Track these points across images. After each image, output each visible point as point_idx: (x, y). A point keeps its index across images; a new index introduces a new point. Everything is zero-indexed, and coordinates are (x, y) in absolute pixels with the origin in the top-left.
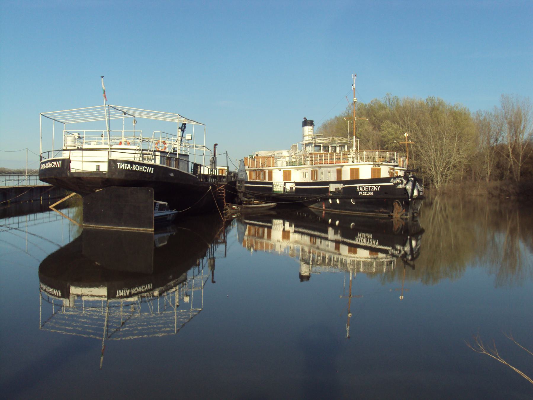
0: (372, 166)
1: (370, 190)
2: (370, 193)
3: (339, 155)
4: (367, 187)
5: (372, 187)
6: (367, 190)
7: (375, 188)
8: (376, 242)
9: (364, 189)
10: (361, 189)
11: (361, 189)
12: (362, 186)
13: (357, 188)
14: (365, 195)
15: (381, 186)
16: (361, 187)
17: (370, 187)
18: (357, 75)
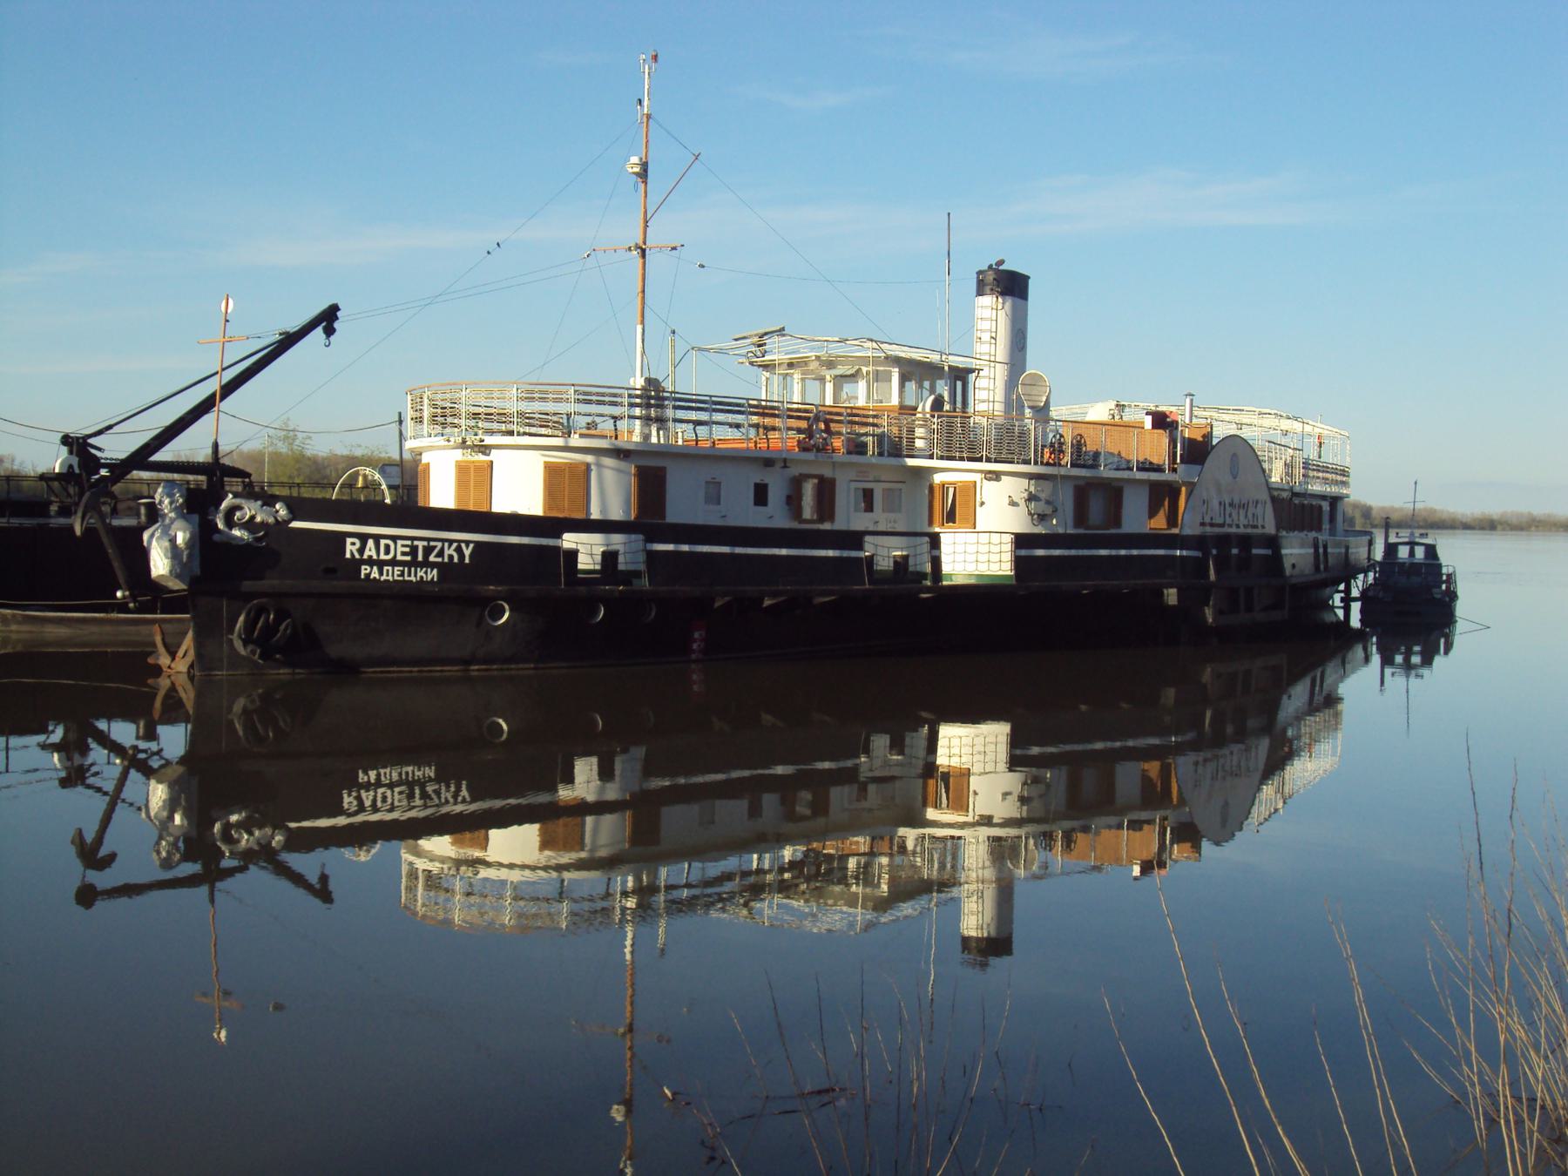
0: (458, 455)
1: (420, 558)
2: (419, 574)
3: (1283, 456)
4: (409, 543)
5: (432, 544)
6: (408, 558)
7: (447, 552)
8: (458, 790)
9: (387, 552)
10: (370, 550)
11: (370, 550)
12: (377, 538)
13: (349, 547)
14: (395, 581)
15: (478, 544)
16: (371, 543)
17: (421, 544)
18: (660, 58)
